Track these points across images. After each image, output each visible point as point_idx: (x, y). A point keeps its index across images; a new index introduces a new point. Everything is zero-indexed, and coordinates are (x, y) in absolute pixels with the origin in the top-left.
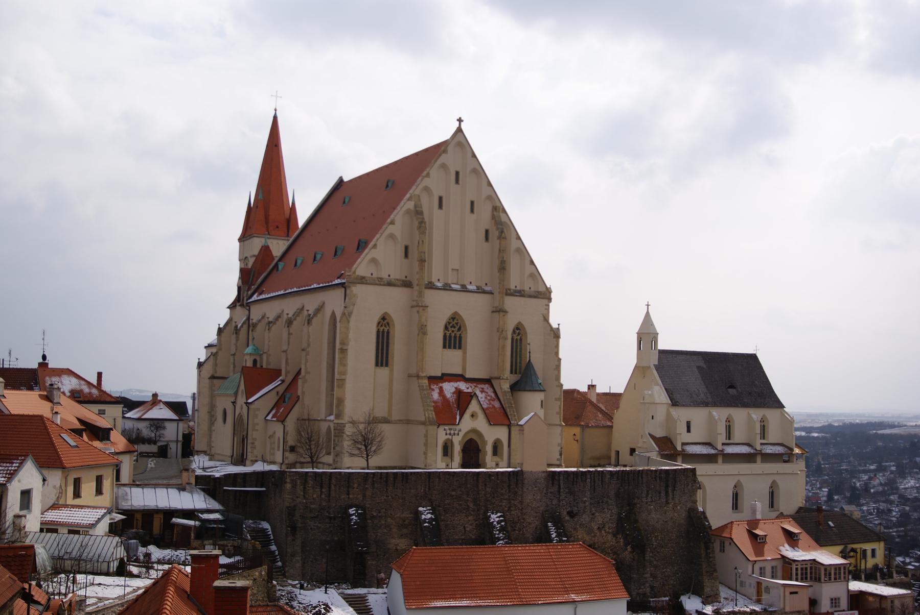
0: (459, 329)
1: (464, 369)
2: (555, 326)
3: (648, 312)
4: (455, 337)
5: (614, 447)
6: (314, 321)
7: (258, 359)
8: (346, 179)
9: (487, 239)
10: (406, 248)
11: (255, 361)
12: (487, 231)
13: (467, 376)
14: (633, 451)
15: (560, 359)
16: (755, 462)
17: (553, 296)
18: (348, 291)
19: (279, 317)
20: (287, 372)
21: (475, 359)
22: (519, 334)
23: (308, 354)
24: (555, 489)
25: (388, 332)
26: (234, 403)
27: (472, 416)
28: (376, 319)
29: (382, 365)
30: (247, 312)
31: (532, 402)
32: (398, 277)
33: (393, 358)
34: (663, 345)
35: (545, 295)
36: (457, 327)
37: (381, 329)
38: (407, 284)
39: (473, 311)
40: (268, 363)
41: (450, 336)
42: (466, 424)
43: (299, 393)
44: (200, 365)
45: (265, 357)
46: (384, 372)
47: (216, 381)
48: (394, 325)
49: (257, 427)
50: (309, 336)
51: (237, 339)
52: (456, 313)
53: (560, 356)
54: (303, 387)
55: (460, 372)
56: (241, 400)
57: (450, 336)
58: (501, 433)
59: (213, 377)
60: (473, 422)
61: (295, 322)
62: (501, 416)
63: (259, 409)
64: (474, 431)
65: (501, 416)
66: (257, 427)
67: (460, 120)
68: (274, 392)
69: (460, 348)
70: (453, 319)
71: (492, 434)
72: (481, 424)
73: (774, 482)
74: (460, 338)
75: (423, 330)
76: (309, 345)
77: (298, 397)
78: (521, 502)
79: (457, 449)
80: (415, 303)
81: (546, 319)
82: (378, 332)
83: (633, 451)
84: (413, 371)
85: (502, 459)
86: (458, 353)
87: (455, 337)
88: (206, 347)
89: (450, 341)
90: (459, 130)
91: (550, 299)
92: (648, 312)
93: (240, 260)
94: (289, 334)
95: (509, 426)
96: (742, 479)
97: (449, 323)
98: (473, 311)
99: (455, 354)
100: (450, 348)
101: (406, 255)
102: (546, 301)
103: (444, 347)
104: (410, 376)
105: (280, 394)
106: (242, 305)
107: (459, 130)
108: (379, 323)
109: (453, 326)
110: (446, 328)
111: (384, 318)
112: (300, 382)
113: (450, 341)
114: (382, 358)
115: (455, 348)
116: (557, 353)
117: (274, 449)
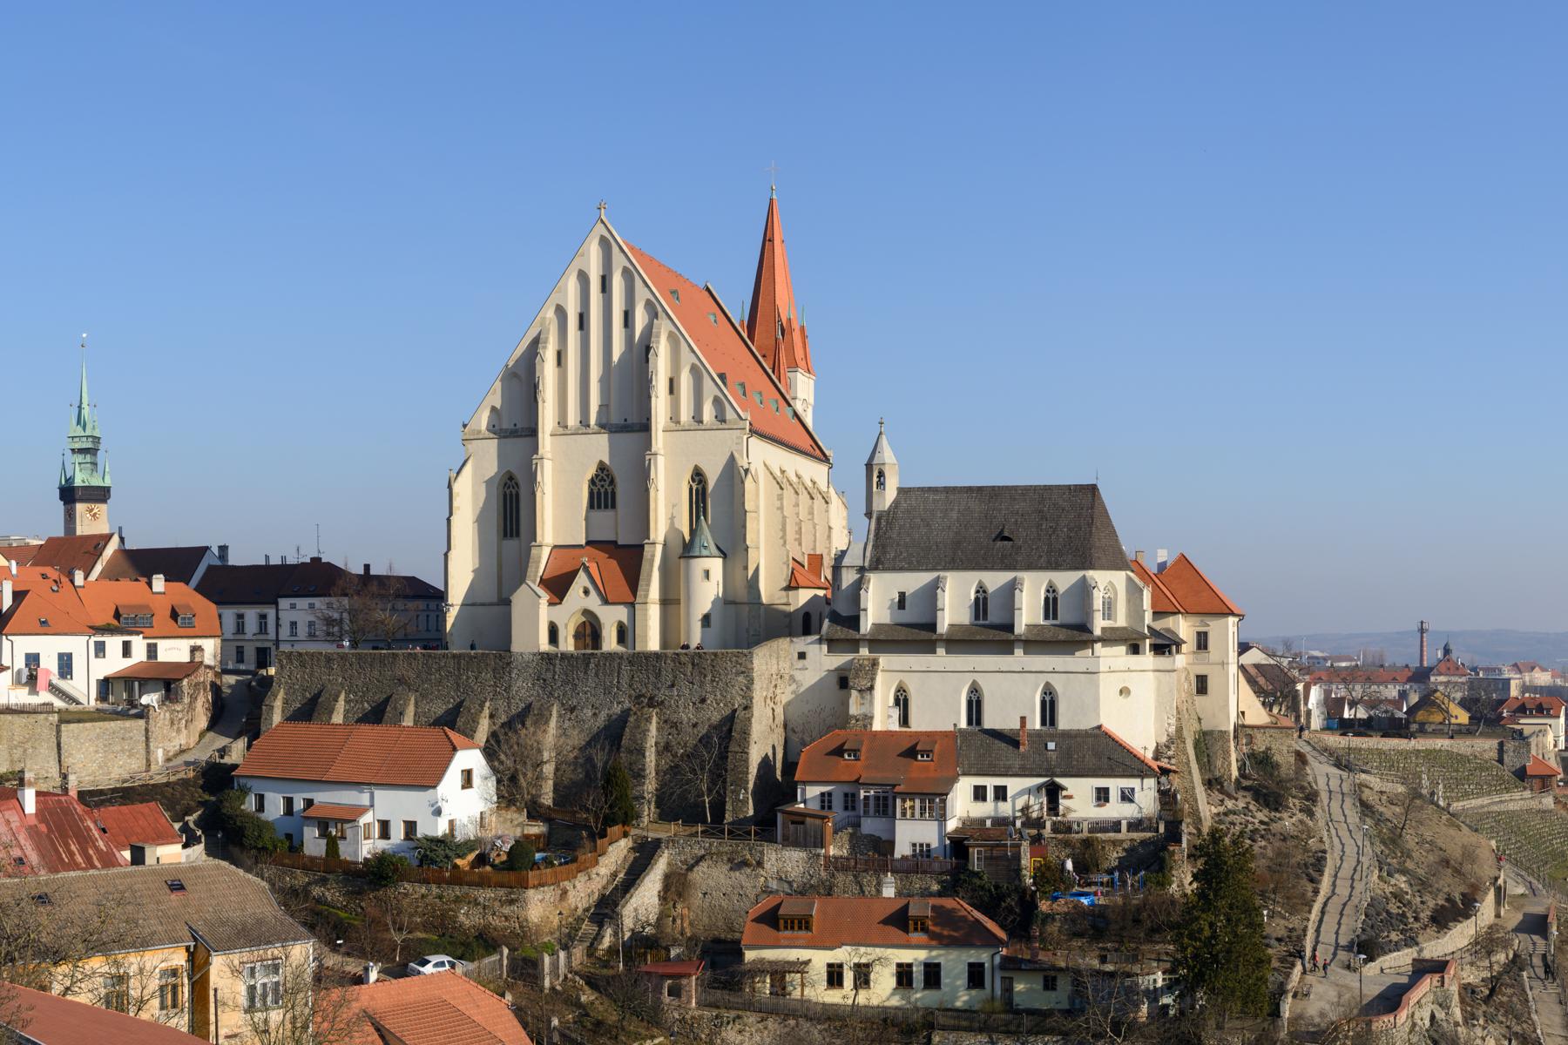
0: (612, 482)
4: (606, 493)
24: (549, 675)
25: (517, 495)
41: (599, 493)
55: (611, 538)
57: (599, 493)
58: (621, 613)
60: (579, 598)
72: (593, 602)
74: (613, 494)
78: (508, 689)
86: (609, 513)
87: (606, 493)
96: (982, 681)
99: (604, 516)
109: (602, 480)
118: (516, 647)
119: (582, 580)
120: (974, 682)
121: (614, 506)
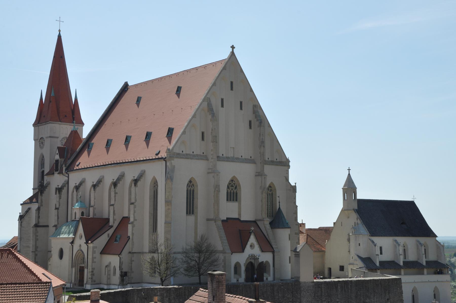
0: (236, 188)
1: (240, 214)
2: (293, 184)
3: (349, 174)
4: (233, 193)
5: (327, 266)
6: (139, 183)
7: (85, 212)
8: (130, 84)
9: (250, 127)
10: (203, 133)
11: (82, 214)
12: (250, 122)
13: (242, 219)
14: (342, 268)
15: (297, 206)
16: (423, 274)
17: (290, 164)
18: (168, 164)
19: (100, 181)
20: (114, 220)
21: (247, 209)
22: (271, 190)
23: (135, 207)
25: (193, 191)
26: (72, 243)
27: (251, 246)
28: (187, 182)
29: (190, 214)
30: (67, 178)
31: (283, 235)
32: (199, 153)
33: (197, 208)
34: (360, 195)
35: (285, 163)
36: (235, 187)
37: (189, 188)
38: (204, 157)
39: (244, 174)
40: (94, 214)
41: (231, 193)
42: (248, 251)
43: (130, 234)
44: (21, 218)
45: (91, 209)
46: (191, 218)
47: (39, 229)
48: (197, 186)
49: (95, 260)
50: (136, 194)
51: (60, 198)
52: (234, 177)
53: (297, 204)
54: (132, 230)
55: (236, 216)
56: (81, 242)
57: (231, 193)
59: (36, 226)
60: (253, 249)
61: (118, 185)
62: (267, 245)
63: (96, 247)
64: (253, 257)
65: (267, 245)
66: (95, 260)
67: (233, 47)
68: (106, 235)
69: (236, 200)
70: (232, 181)
71: (266, 257)
72: (256, 251)
73: (436, 288)
74: (236, 193)
75: (217, 188)
76: (136, 200)
77: (129, 237)
79: (243, 268)
80: (210, 171)
81: (287, 179)
82: (187, 190)
83: (342, 268)
84: (212, 217)
85: (270, 275)
86: (235, 204)
87: (233, 193)
88: (21, 204)
89: (230, 195)
90: (233, 54)
91: (289, 166)
92: (349, 174)
93: (34, 140)
94: (116, 193)
95: (273, 252)
97: (230, 184)
98: (244, 174)
99: (233, 205)
100: (230, 200)
101: (203, 139)
102: (286, 168)
103: (227, 200)
104: (208, 220)
105: (110, 235)
106: (61, 173)
107: (233, 54)
108: (188, 185)
109: (232, 186)
110: (228, 187)
111: (190, 182)
112: (130, 226)
113: (230, 195)
114: (191, 209)
115: (233, 200)
116: (295, 203)
117: (110, 275)
118: (302, 280)
119: (252, 240)
120: (436, 288)
121: (236, 200)
